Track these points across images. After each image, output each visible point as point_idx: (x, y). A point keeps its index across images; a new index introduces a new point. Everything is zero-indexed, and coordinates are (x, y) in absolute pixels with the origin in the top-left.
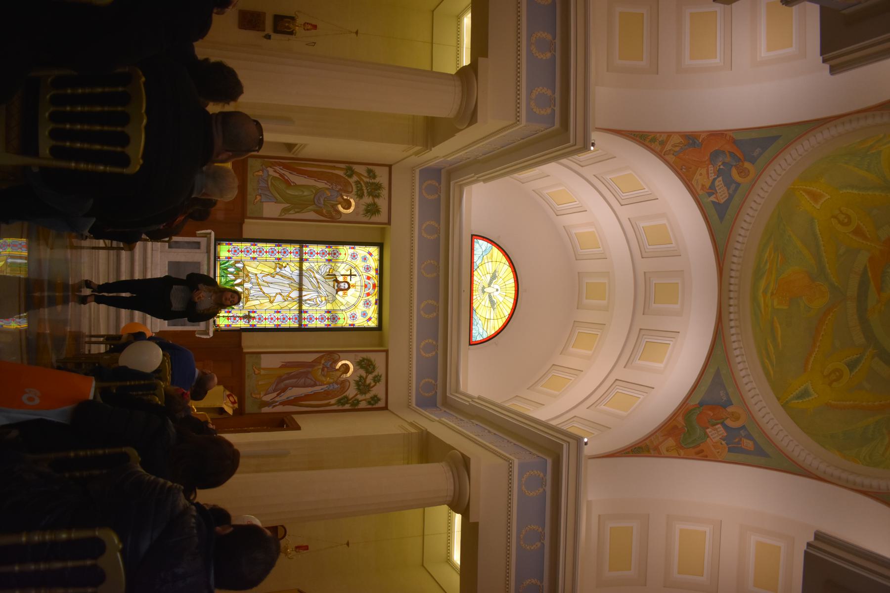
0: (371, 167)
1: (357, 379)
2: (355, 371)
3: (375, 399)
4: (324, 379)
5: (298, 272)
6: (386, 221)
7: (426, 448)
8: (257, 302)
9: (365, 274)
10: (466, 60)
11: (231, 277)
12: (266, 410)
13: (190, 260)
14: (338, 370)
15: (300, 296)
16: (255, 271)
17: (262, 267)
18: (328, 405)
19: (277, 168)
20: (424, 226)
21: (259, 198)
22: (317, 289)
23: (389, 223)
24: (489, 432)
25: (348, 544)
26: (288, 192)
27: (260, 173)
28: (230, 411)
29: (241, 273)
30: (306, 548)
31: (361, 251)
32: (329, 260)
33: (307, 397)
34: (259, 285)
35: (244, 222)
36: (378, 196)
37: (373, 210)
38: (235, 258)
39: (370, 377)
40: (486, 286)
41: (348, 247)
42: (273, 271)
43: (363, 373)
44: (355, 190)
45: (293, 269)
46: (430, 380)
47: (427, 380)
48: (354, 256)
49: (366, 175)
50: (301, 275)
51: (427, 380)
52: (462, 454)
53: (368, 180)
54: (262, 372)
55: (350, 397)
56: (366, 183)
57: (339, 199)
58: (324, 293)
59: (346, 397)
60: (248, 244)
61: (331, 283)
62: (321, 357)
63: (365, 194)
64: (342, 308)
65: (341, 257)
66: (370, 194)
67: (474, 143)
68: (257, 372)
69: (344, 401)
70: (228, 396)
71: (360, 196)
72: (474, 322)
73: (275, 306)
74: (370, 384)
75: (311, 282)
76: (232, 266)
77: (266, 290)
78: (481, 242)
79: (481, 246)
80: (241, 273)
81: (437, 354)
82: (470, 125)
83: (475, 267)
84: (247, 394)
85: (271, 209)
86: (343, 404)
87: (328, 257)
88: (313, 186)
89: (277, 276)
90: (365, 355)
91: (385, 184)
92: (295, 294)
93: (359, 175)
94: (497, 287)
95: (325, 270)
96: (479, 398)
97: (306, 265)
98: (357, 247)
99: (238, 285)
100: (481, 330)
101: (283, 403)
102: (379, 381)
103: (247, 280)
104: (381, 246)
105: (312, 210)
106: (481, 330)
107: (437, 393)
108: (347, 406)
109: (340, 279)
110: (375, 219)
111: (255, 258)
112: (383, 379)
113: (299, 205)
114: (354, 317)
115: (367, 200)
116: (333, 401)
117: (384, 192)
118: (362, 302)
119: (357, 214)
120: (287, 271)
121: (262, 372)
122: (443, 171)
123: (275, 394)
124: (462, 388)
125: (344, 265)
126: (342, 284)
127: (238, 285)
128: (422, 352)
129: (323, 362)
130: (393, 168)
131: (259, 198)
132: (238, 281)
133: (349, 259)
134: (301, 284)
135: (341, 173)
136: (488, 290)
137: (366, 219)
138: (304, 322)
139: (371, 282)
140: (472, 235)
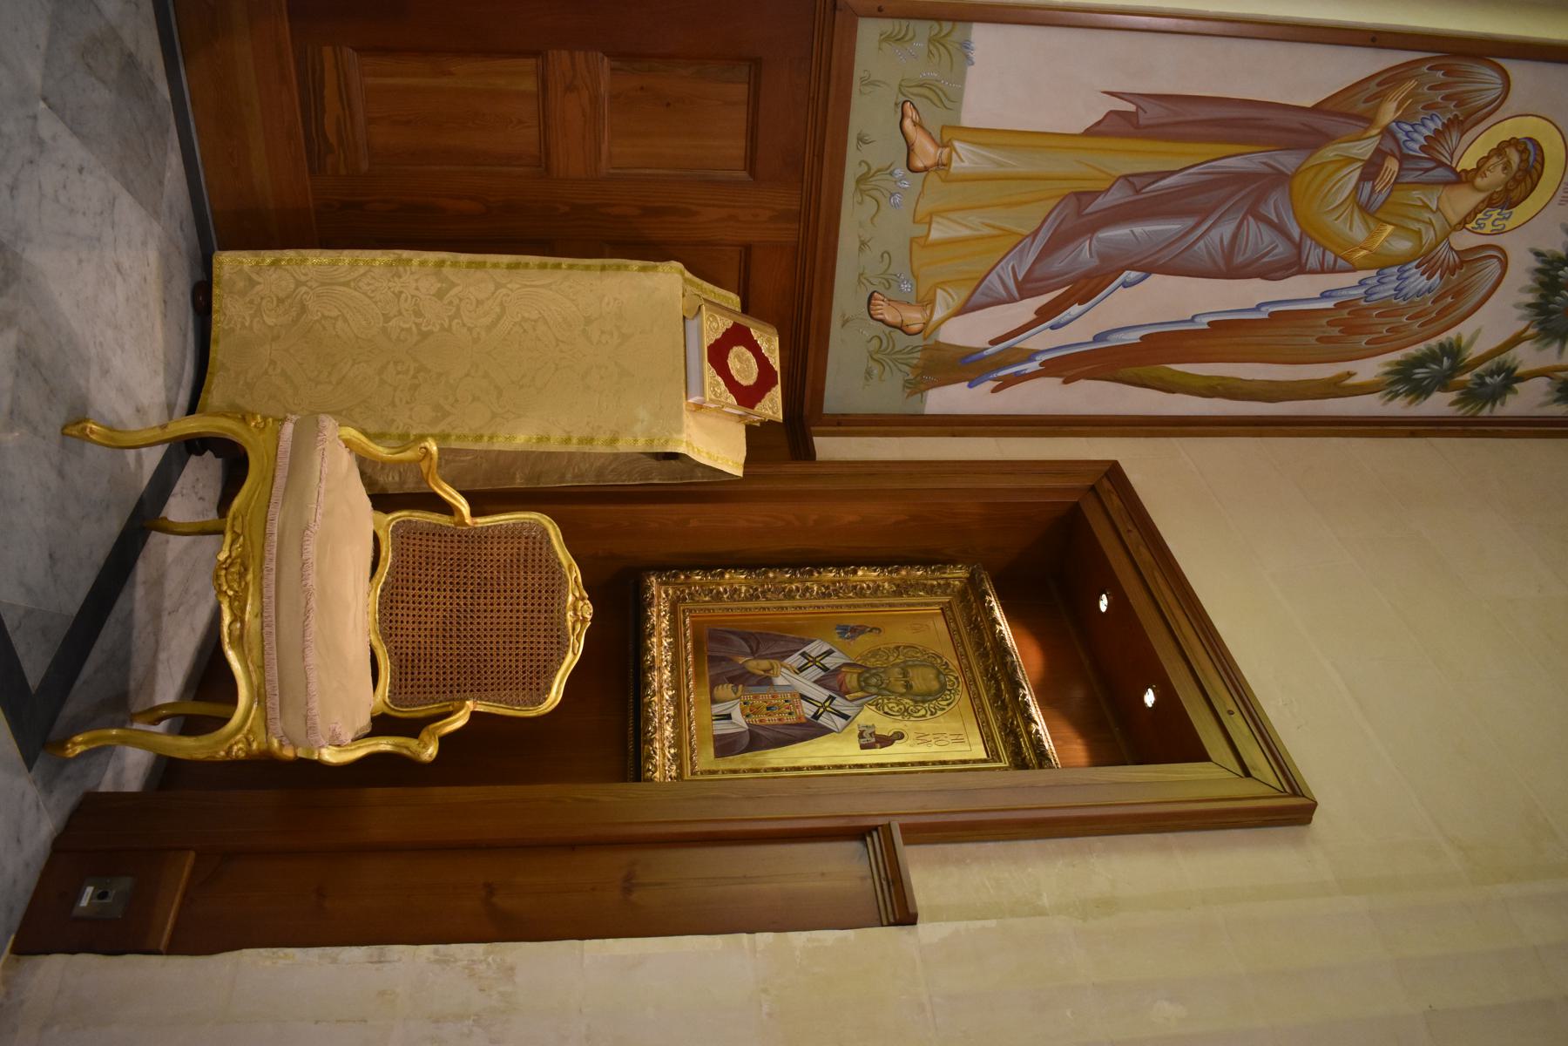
4: (1359, 232)
14: (1463, 179)
18: (1335, 388)
28: (717, 446)
33: (1226, 336)
54: (966, 158)
55: (1476, 351)
59: (1453, 351)
62: (1388, 80)
68: (927, 152)
70: (718, 354)
84: (846, 298)
86: (1420, 391)
101: (1067, 367)
108: (1439, 404)
116: (1369, 369)
121: (966, 158)
123: (1026, 309)
129: (1389, 113)
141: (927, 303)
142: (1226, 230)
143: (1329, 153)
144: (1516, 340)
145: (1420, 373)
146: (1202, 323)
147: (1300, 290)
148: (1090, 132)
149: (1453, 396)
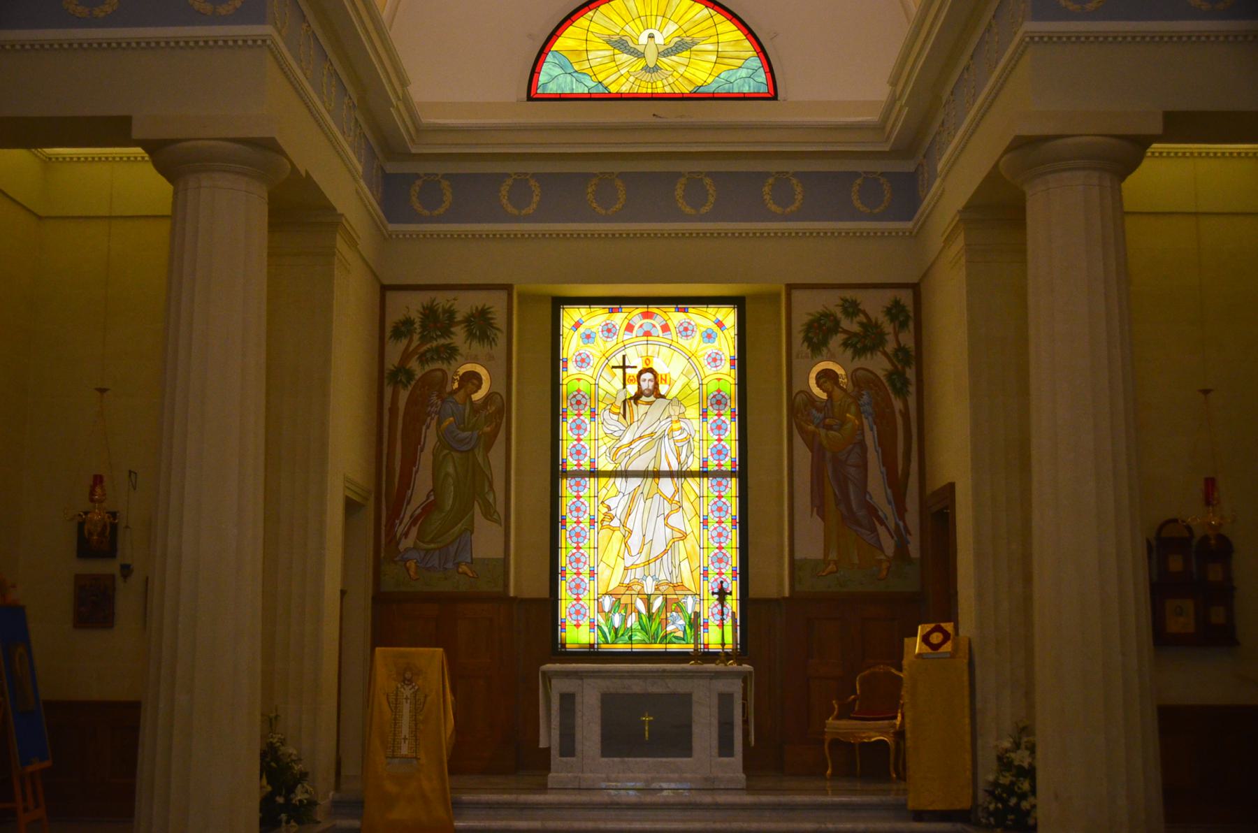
0: (386, 330)
1: (849, 352)
2: (832, 358)
3: (895, 311)
4: (849, 426)
5: (618, 480)
6: (503, 295)
7: (999, 212)
8: (685, 567)
9: (623, 335)
10: (138, 151)
11: (632, 621)
12: (914, 549)
13: (598, 713)
14: (830, 396)
15: (671, 474)
16: (619, 571)
17: (610, 556)
18: (906, 416)
19: (400, 530)
20: (511, 209)
21: (463, 568)
22: (655, 439)
23: (508, 288)
24: (967, 68)
25: (1206, 392)
26: (449, 503)
27: (412, 565)
29: (624, 600)
30: (1210, 484)
31: (571, 345)
32: (593, 414)
34: (648, 562)
35: (515, 599)
36: (450, 313)
37: (480, 326)
38: (592, 612)
39: (845, 324)
40: (642, 63)
41: (563, 374)
42: (618, 535)
43: (836, 341)
44: (438, 365)
45: (613, 492)
46: (855, 188)
47: (855, 197)
48: (583, 361)
49: (405, 342)
50: (626, 474)
51: (855, 197)
52: (1008, 150)
53: (416, 337)
54: (833, 556)
55: (889, 366)
56: (424, 339)
57: (459, 397)
58: (665, 425)
59: (890, 376)
60: (563, 586)
61: (642, 408)
62: (802, 432)
63: (447, 341)
64: (695, 385)
65: (583, 386)
66: (447, 332)
67: (320, 124)
68: (832, 567)
69: (898, 381)
71: (450, 353)
72: (725, 89)
73: (693, 527)
74: (861, 324)
75: (640, 453)
76: (608, 619)
77: (658, 548)
78: (543, 78)
79: (552, 78)
80: (624, 600)
81: (796, 174)
82: (282, 152)
83: (601, 90)
85: (486, 542)
86: (906, 382)
87: (586, 416)
88: (435, 455)
89: (630, 525)
90: (798, 337)
91: (423, 298)
92: (667, 485)
93: (406, 356)
94: (643, 39)
95: (612, 422)
96: (894, 83)
97: (604, 464)
98: (564, 354)
99: (649, 605)
100: (743, 73)
101: (901, 510)
102: (854, 304)
103: (637, 588)
104: (560, 302)
105: (486, 456)
106: (743, 73)
107: (880, 174)
108: (910, 373)
109: (632, 389)
110: (499, 319)
111: (592, 574)
112: (849, 294)
113: (475, 486)
114: (714, 360)
115: (459, 336)
116: (898, 404)
117: (442, 300)
118: (683, 341)
119: (491, 358)
120: (618, 506)
122: (391, 168)
123: (881, 530)
124: (872, 117)
125: (602, 383)
126: (644, 386)
127: (649, 605)
128: (793, 208)
129: (811, 428)
130: (386, 282)
131: (463, 568)
132: (641, 606)
133: (589, 371)
134: (644, 474)
135: (404, 395)
136: (651, 59)
137: (501, 339)
138: (727, 465)
139: (638, 321)
140: (530, 98)
141: (880, 561)
142: (852, 470)
143: (825, 442)
144: (885, 354)
145: (899, 385)
146: (883, 469)
147: (870, 439)
148: (823, 518)
149: (908, 370)
